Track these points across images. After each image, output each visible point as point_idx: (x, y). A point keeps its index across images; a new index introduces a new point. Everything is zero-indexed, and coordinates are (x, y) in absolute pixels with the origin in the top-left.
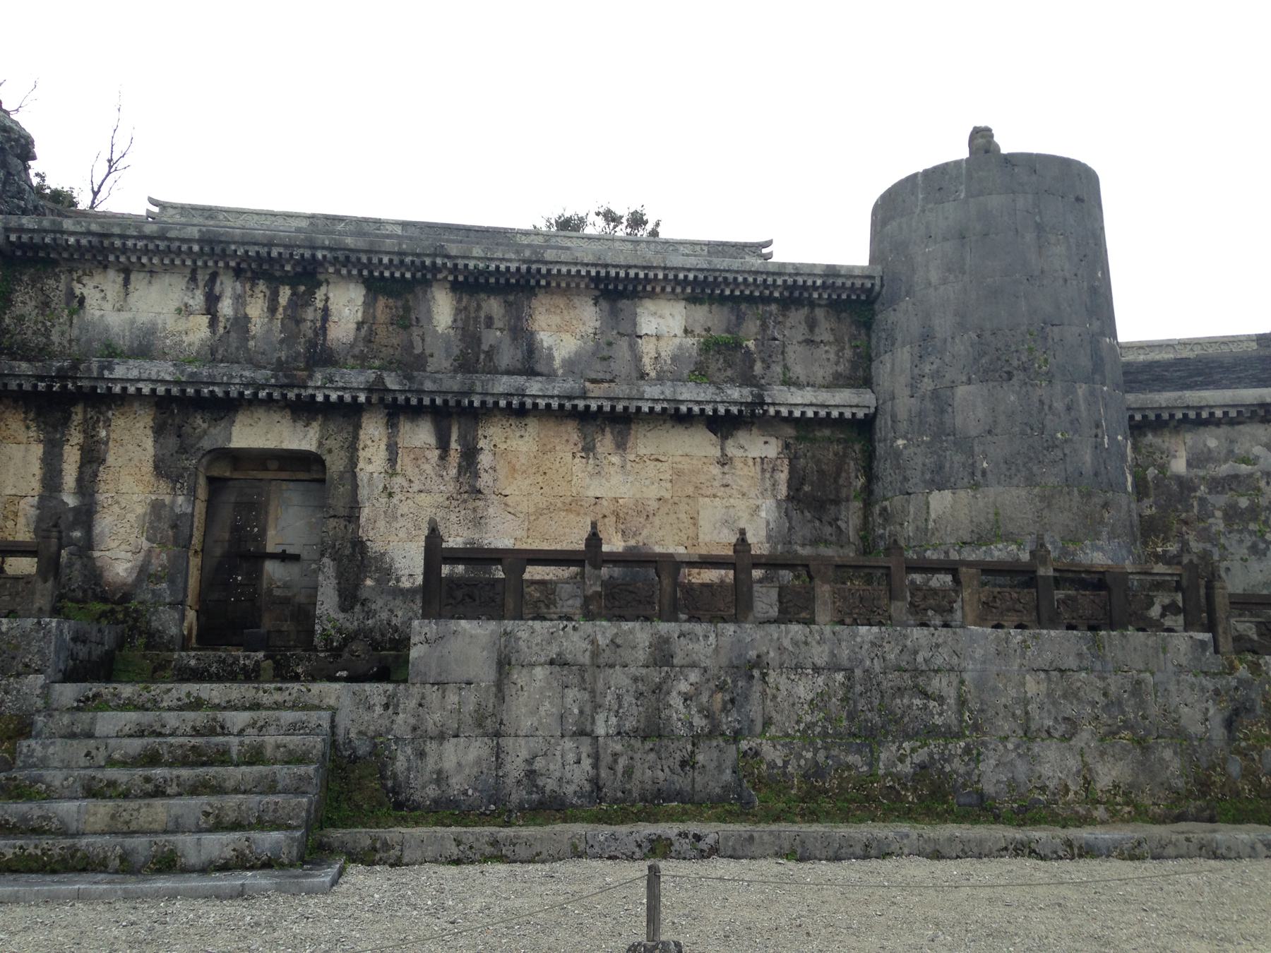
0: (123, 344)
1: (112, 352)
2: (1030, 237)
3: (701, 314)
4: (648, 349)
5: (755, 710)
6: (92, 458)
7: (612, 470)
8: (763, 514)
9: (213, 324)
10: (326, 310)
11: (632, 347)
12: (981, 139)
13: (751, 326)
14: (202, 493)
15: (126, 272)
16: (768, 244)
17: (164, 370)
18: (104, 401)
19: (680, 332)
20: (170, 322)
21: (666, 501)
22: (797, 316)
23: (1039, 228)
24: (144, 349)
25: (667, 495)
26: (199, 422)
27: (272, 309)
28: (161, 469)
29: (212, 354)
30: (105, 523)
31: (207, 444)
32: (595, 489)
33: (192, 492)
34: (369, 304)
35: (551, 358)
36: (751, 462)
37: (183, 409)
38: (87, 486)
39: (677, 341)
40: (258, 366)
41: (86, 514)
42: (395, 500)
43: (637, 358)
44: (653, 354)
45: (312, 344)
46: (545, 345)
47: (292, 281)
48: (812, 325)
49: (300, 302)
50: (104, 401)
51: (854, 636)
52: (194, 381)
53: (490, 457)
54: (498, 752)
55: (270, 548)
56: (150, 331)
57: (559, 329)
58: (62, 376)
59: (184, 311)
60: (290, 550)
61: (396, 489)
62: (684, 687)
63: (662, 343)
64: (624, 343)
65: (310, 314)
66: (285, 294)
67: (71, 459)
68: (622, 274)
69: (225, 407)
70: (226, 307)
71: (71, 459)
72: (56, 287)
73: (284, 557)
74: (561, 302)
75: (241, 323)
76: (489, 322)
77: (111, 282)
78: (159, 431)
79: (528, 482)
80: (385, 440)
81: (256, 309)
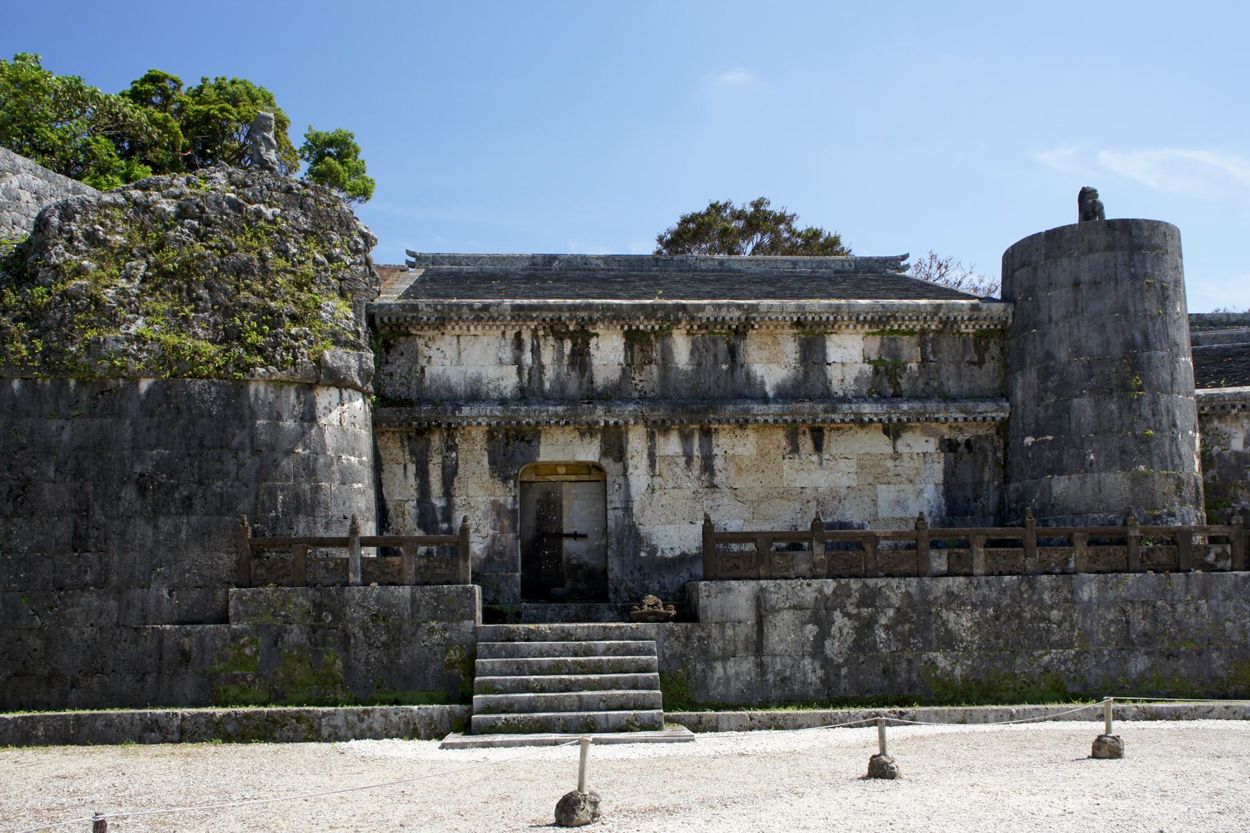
4: (834, 373)
7: (812, 467)
8: (926, 495)
9: (520, 372)
12: (1088, 202)
19: (860, 359)
21: (853, 488)
25: (854, 484)
29: (525, 394)
32: (801, 480)
35: (763, 383)
36: (915, 457)
39: (858, 366)
42: (656, 495)
44: (840, 377)
46: (759, 374)
51: (1000, 582)
53: (723, 461)
54: (761, 666)
55: (565, 531)
57: (769, 361)
60: (580, 531)
61: (657, 487)
62: (883, 621)
63: (847, 368)
66: (568, 345)
68: (817, 318)
70: (528, 358)
73: (575, 536)
79: (751, 478)
80: (646, 451)
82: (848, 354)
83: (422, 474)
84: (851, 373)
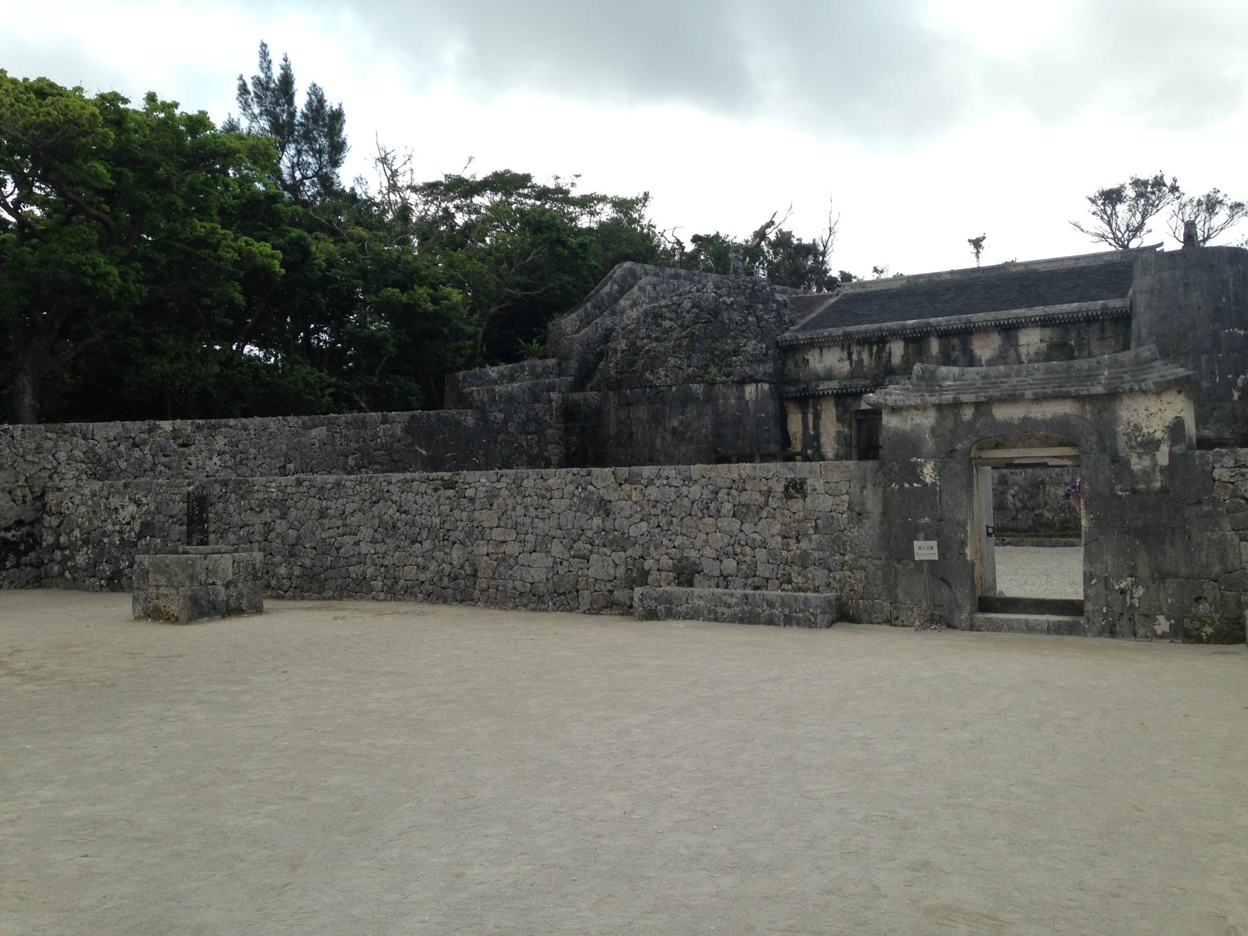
0: (822, 375)
1: (820, 379)
2: (1181, 290)
3: (1048, 332)
4: (1023, 351)
5: (1041, 499)
6: (817, 417)
10: (890, 353)
11: (1016, 351)
13: (1073, 334)
14: (854, 425)
15: (821, 348)
16: (1161, 244)
17: (834, 384)
18: (819, 397)
20: (838, 365)
22: (1095, 328)
23: (1186, 285)
24: (829, 376)
26: (849, 401)
27: (871, 355)
28: (839, 419)
29: (851, 375)
30: (823, 439)
31: (852, 408)
33: (850, 427)
34: (906, 348)
37: (845, 398)
38: (816, 427)
40: (867, 378)
41: (817, 437)
43: (1019, 356)
45: (886, 366)
47: (876, 343)
48: (1102, 330)
49: (880, 350)
50: (819, 397)
52: (846, 387)
56: (831, 369)
58: (804, 390)
59: (841, 360)
64: (1012, 350)
65: (884, 355)
66: (875, 348)
67: (810, 417)
69: (858, 395)
70: (855, 357)
71: (810, 417)
72: (799, 357)
74: (984, 335)
75: (861, 361)
76: (954, 347)
77: (816, 353)
78: (836, 405)
81: (865, 356)
82: (1031, 340)
83: (805, 421)
84: (1032, 350)
